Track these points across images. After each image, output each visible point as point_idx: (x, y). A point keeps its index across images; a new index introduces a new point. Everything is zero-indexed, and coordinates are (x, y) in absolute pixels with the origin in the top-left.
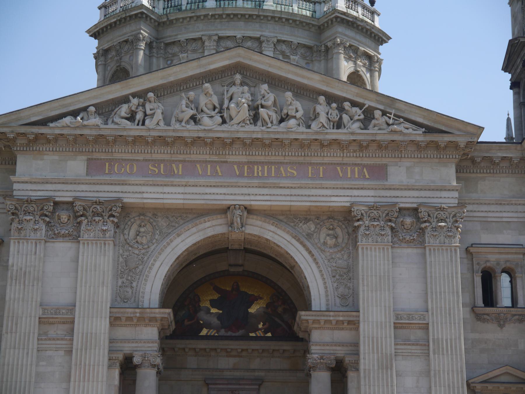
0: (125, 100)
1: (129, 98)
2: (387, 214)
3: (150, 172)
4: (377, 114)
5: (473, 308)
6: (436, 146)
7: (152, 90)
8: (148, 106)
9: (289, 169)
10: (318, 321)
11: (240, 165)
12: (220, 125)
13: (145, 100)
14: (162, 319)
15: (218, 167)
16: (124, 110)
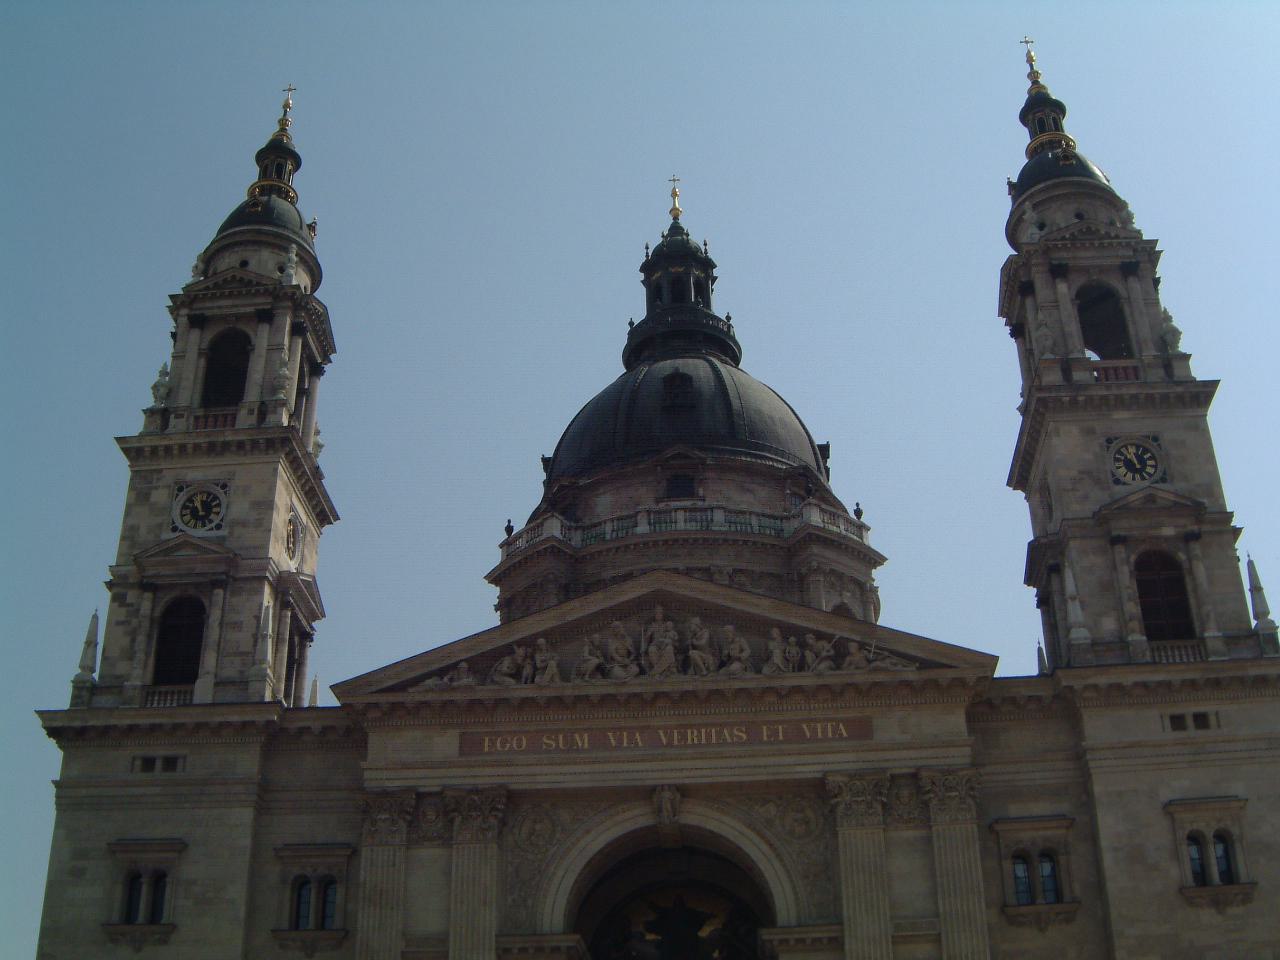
0: (508, 650)
1: (512, 649)
2: (876, 786)
3: (544, 747)
4: (853, 647)
5: (1003, 908)
6: (935, 684)
7: (545, 634)
8: (538, 658)
9: (736, 732)
10: (785, 941)
12: (637, 676)
13: (534, 650)
14: (569, 948)
15: (637, 735)
16: (506, 664)
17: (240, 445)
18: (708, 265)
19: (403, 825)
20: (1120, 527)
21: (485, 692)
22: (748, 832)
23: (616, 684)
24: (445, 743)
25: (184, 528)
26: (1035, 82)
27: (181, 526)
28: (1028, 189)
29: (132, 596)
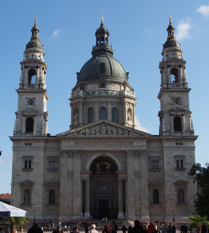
0: (82, 130)
5: (150, 169)
7: (86, 128)
11: (104, 142)
17: (37, 92)
18: (108, 34)
19: (67, 156)
20: (172, 113)
21: (79, 136)
22: (115, 157)
23: (96, 136)
24: (72, 143)
25: (28, 105)
26: (170, 23)
27: (28, 105)
28: (165, 48)
29: (21, 117)
